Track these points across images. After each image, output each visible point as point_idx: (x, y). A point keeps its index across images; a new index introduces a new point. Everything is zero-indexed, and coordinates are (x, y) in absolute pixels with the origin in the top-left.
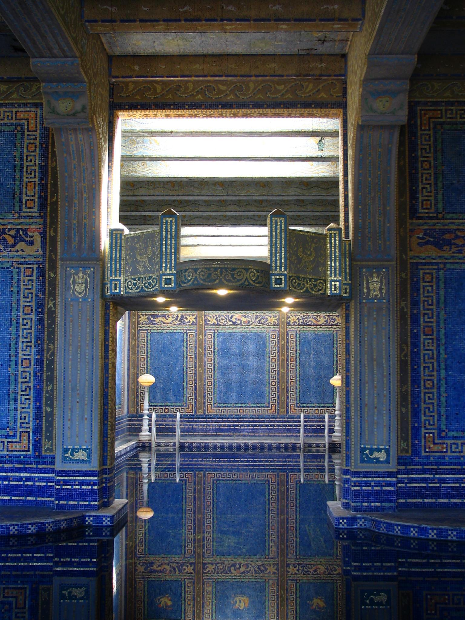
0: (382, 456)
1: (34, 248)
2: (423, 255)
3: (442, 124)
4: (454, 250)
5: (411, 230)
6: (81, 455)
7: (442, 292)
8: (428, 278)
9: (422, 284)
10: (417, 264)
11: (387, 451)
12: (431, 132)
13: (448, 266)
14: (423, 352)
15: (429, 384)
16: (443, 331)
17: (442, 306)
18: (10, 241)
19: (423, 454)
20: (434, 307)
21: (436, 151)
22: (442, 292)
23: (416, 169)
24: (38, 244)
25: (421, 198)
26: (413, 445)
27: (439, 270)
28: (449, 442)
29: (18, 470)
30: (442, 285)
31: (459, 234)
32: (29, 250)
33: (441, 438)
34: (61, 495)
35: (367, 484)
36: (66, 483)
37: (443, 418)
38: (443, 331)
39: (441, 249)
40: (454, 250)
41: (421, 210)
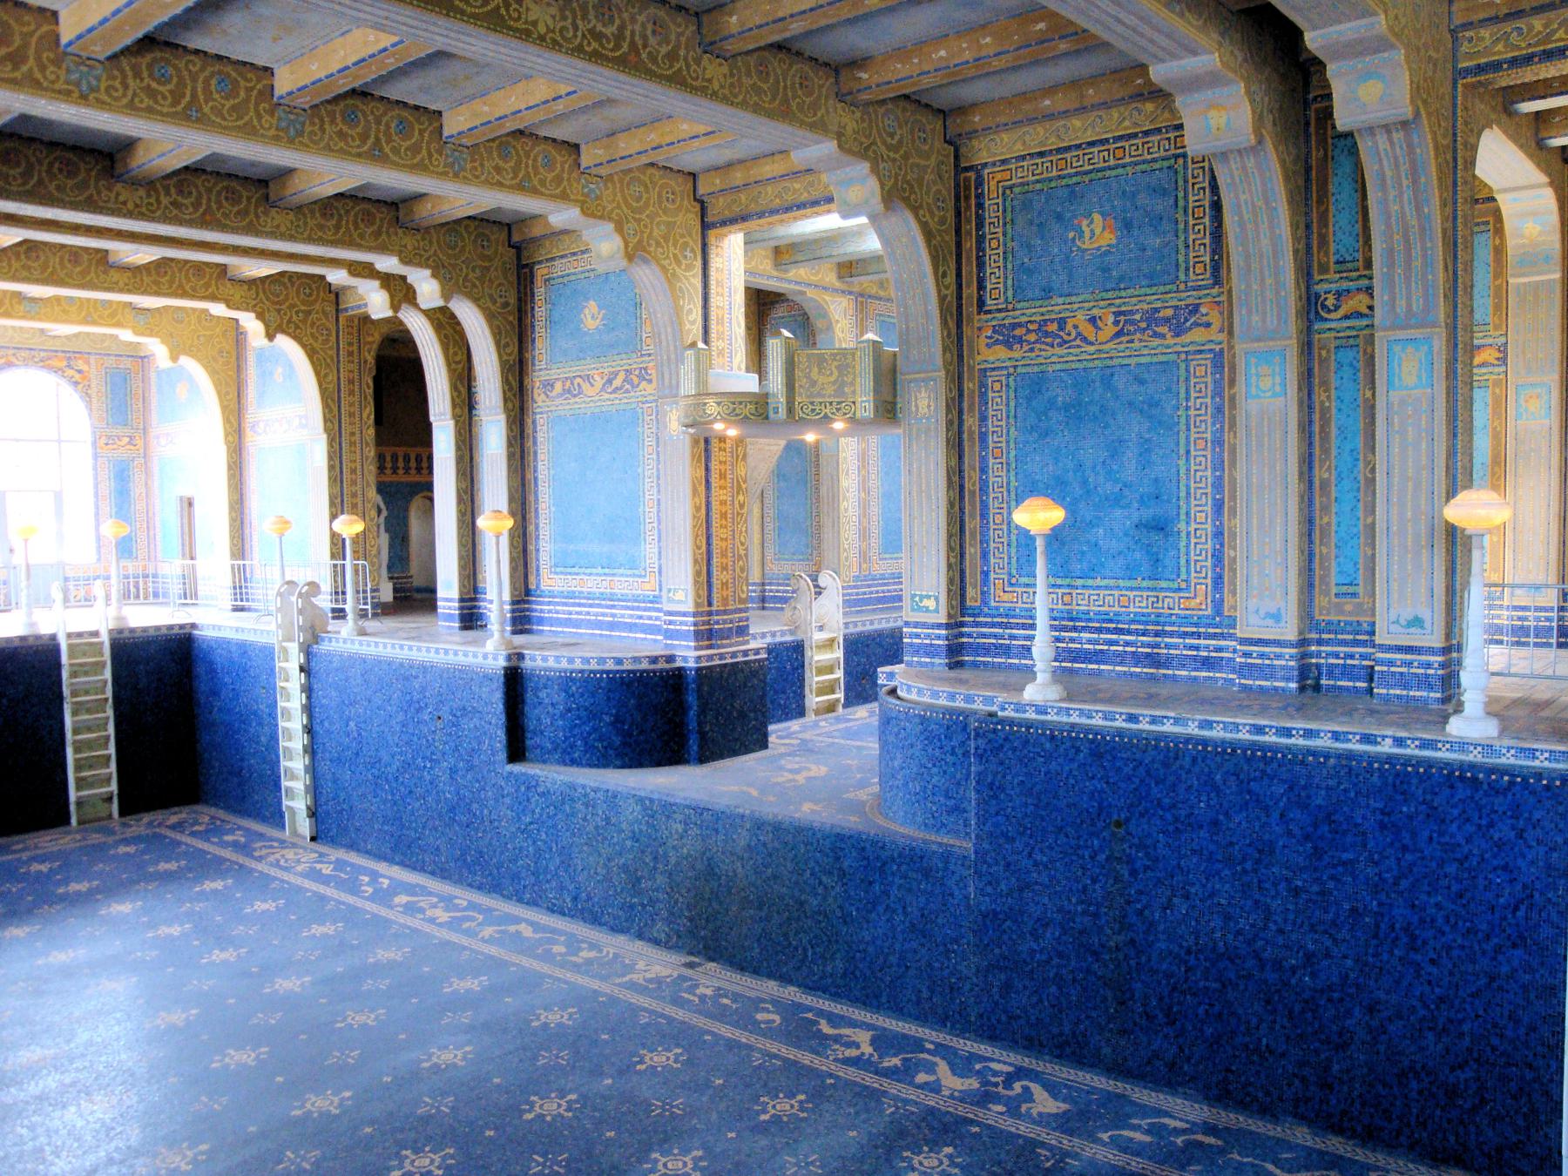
0: (931, 604)
1: (654, 384)
2: (991, 359)
3: (1011, 188)
4: (1026, 348)
5: (980, 329)
6: (680, 596)
7: (1012, 404)
8: (997, 386)
9: (990, 395)
10: (985, 370)
11: (937, 599)
12: (1000, 201)
13: (1019, 370)
14: (992, 480)
15: (998, 519)
16: (1013, 453)
17: (1012, 420)
18: (636, 381)
19: (993, 604)
20: (1003, 423)
21: (1005, 224)
22: (1012, 404)
23: (984, 250)
24: (654, 384)
25: (989, 287)
26: (983, 593)
27: (1009, 375)
28: (1020, 590)
29: (649, 609)
30: (1012, 395)
31: (1031, 327)
32: (650, 388)
33: (1011, 585)
34: (669, 635)
35: (918, 636)
36: (671, 623)
37: (1014, 561)
38: (1013, 453)
39: (1011, 349)
40: (1026, 348)
41: (989, 302)
